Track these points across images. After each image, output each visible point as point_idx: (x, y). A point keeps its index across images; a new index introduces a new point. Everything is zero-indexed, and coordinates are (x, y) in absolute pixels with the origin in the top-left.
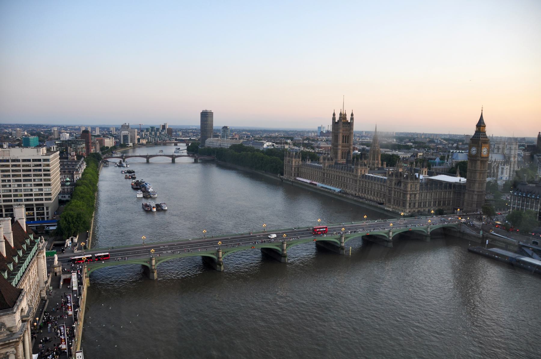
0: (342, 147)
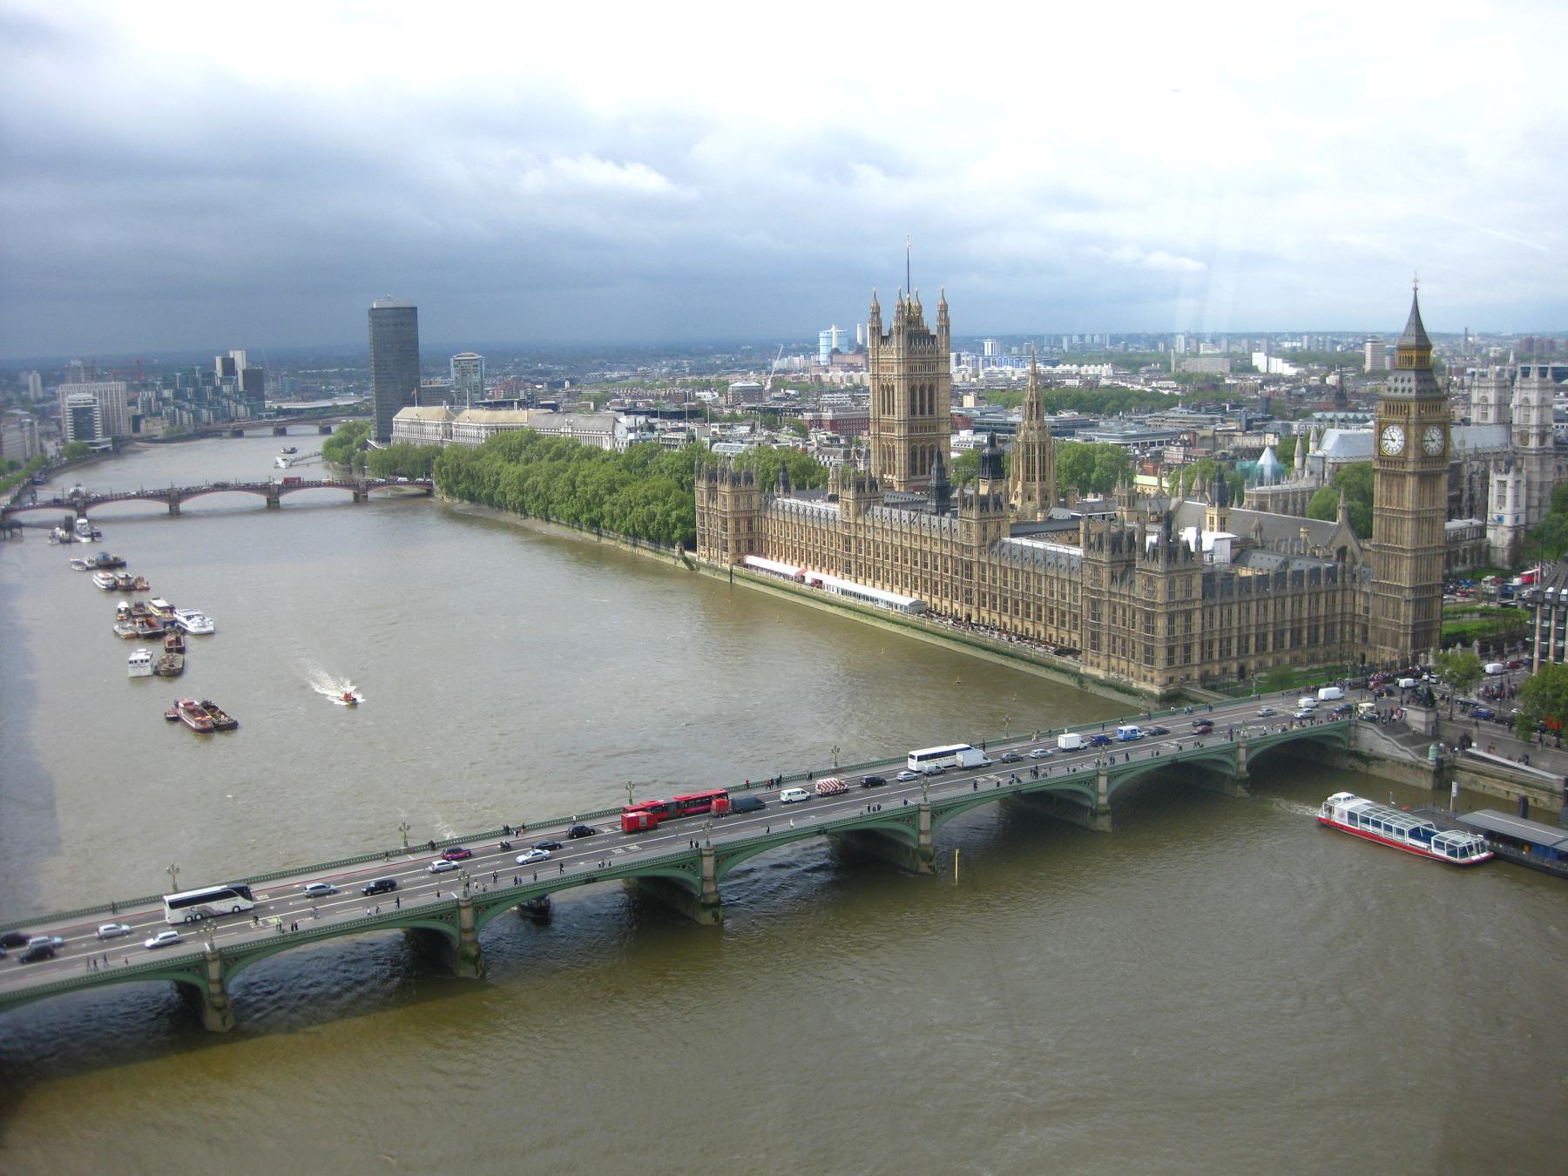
0: (911, 429)
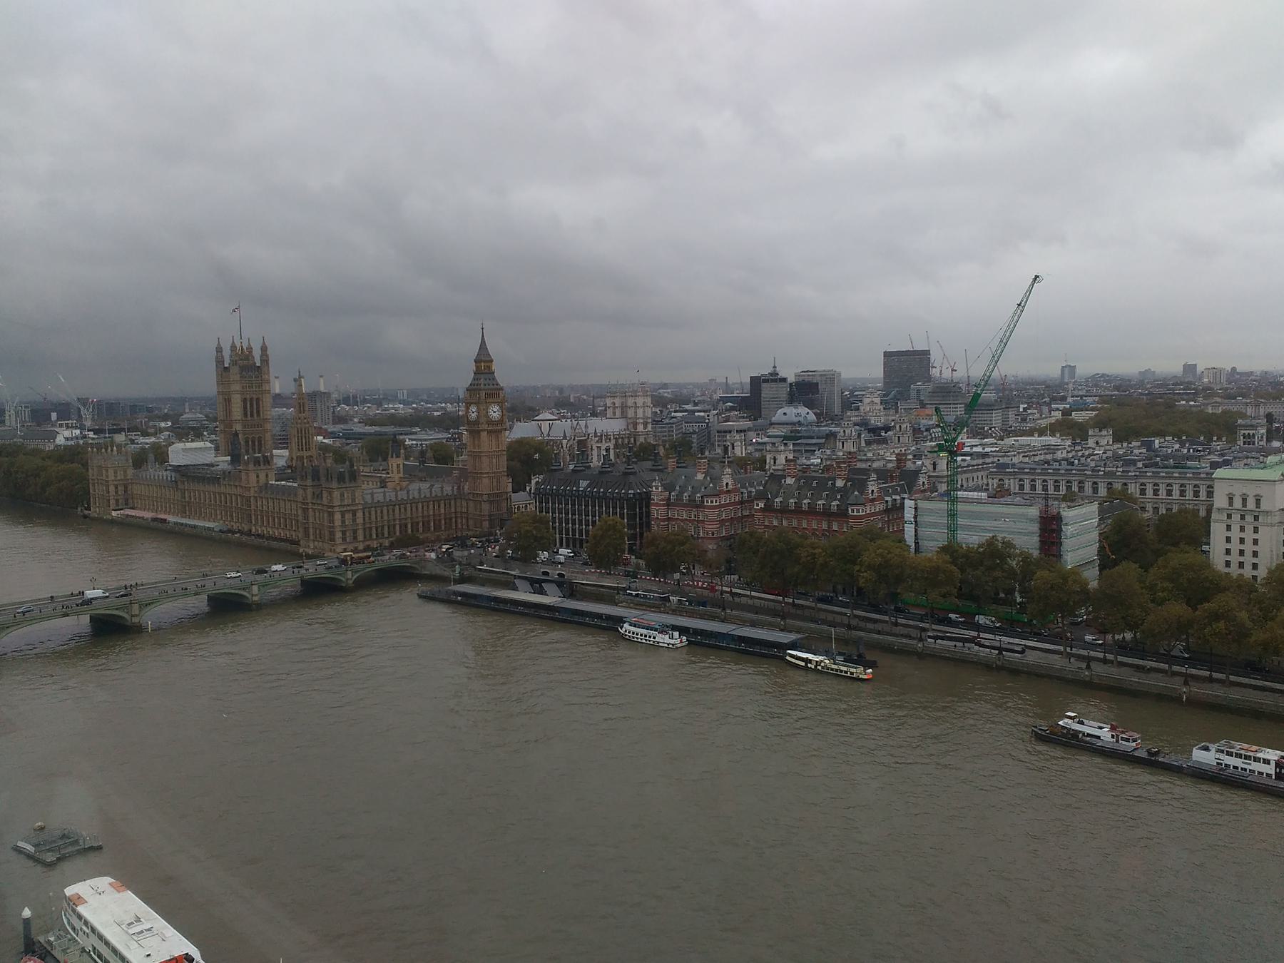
0: (245, 426)
